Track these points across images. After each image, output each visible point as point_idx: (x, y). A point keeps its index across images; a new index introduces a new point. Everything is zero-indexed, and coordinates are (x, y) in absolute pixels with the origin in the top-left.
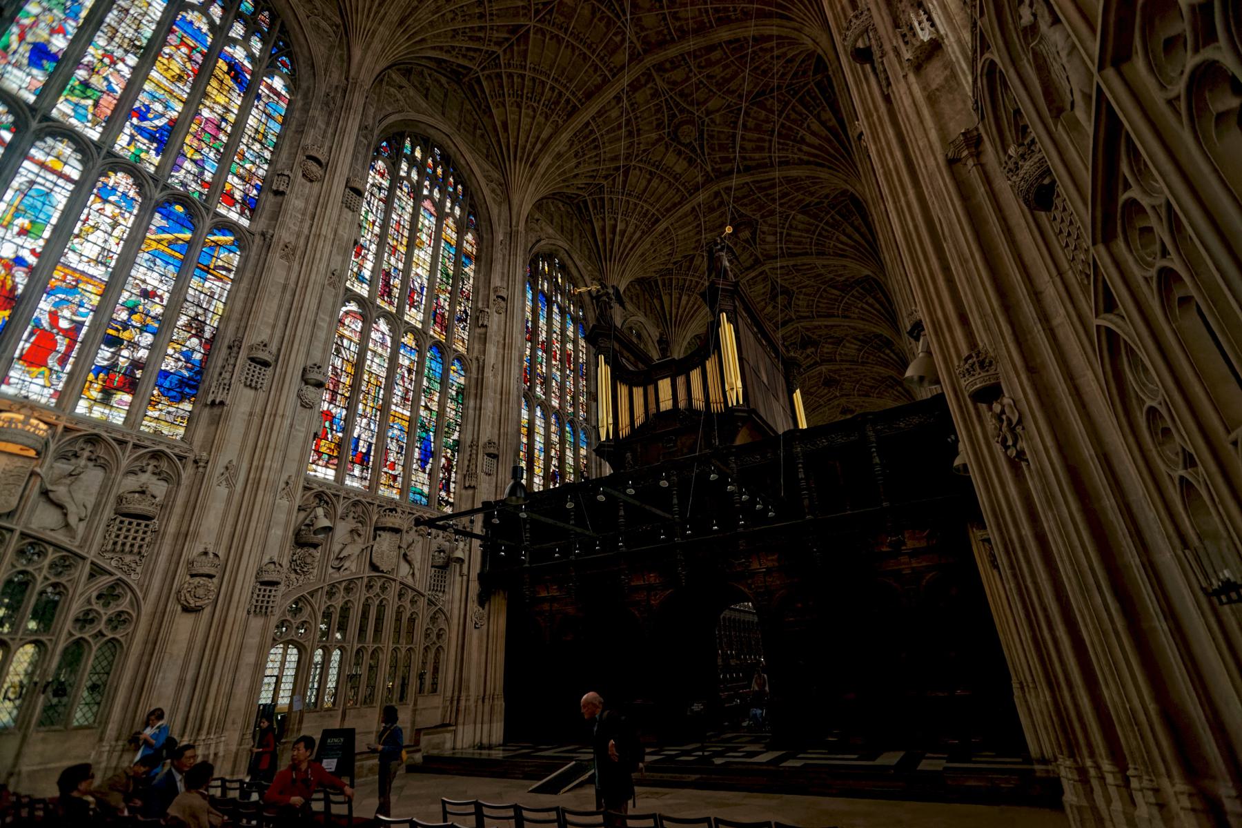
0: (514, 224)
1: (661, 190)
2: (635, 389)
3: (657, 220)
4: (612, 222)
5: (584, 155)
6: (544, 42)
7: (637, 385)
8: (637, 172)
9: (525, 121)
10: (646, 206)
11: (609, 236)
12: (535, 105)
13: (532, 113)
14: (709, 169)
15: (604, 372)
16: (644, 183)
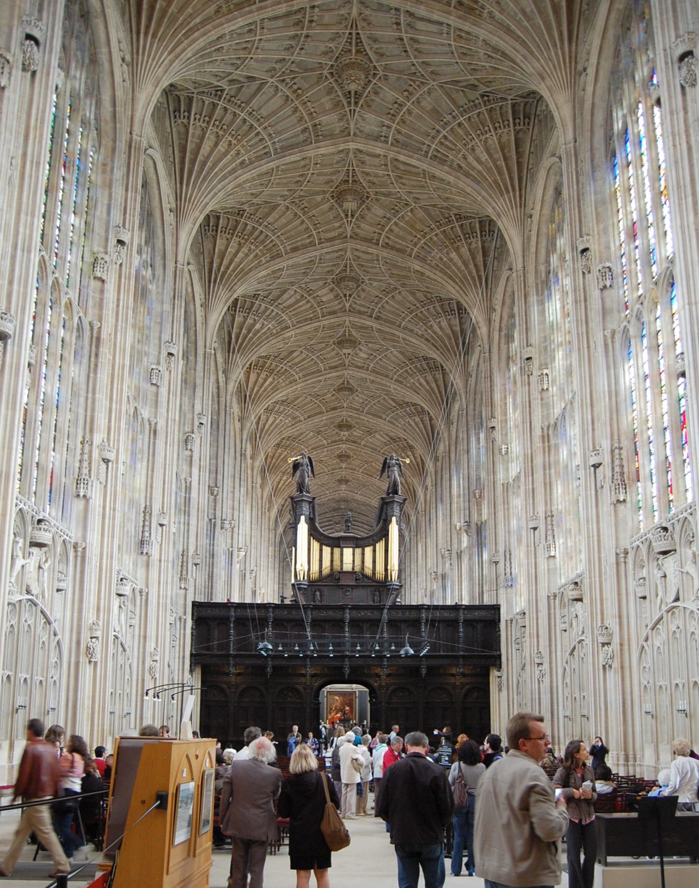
0: (208, 345)
1: (302, 309)
2: (324, 547)
3: (287, 328)
4: (251, 321)
5: (265, 281)
6: (285, 213)
7: (327, 545)
8: (292, 293)
9: (240, 255)
10: (285, 317)
11: (244, 331)
12: (253, 247)
13: (246, 251)
14: (347, 305)
15: (303, 528)
16: (293, 300)
